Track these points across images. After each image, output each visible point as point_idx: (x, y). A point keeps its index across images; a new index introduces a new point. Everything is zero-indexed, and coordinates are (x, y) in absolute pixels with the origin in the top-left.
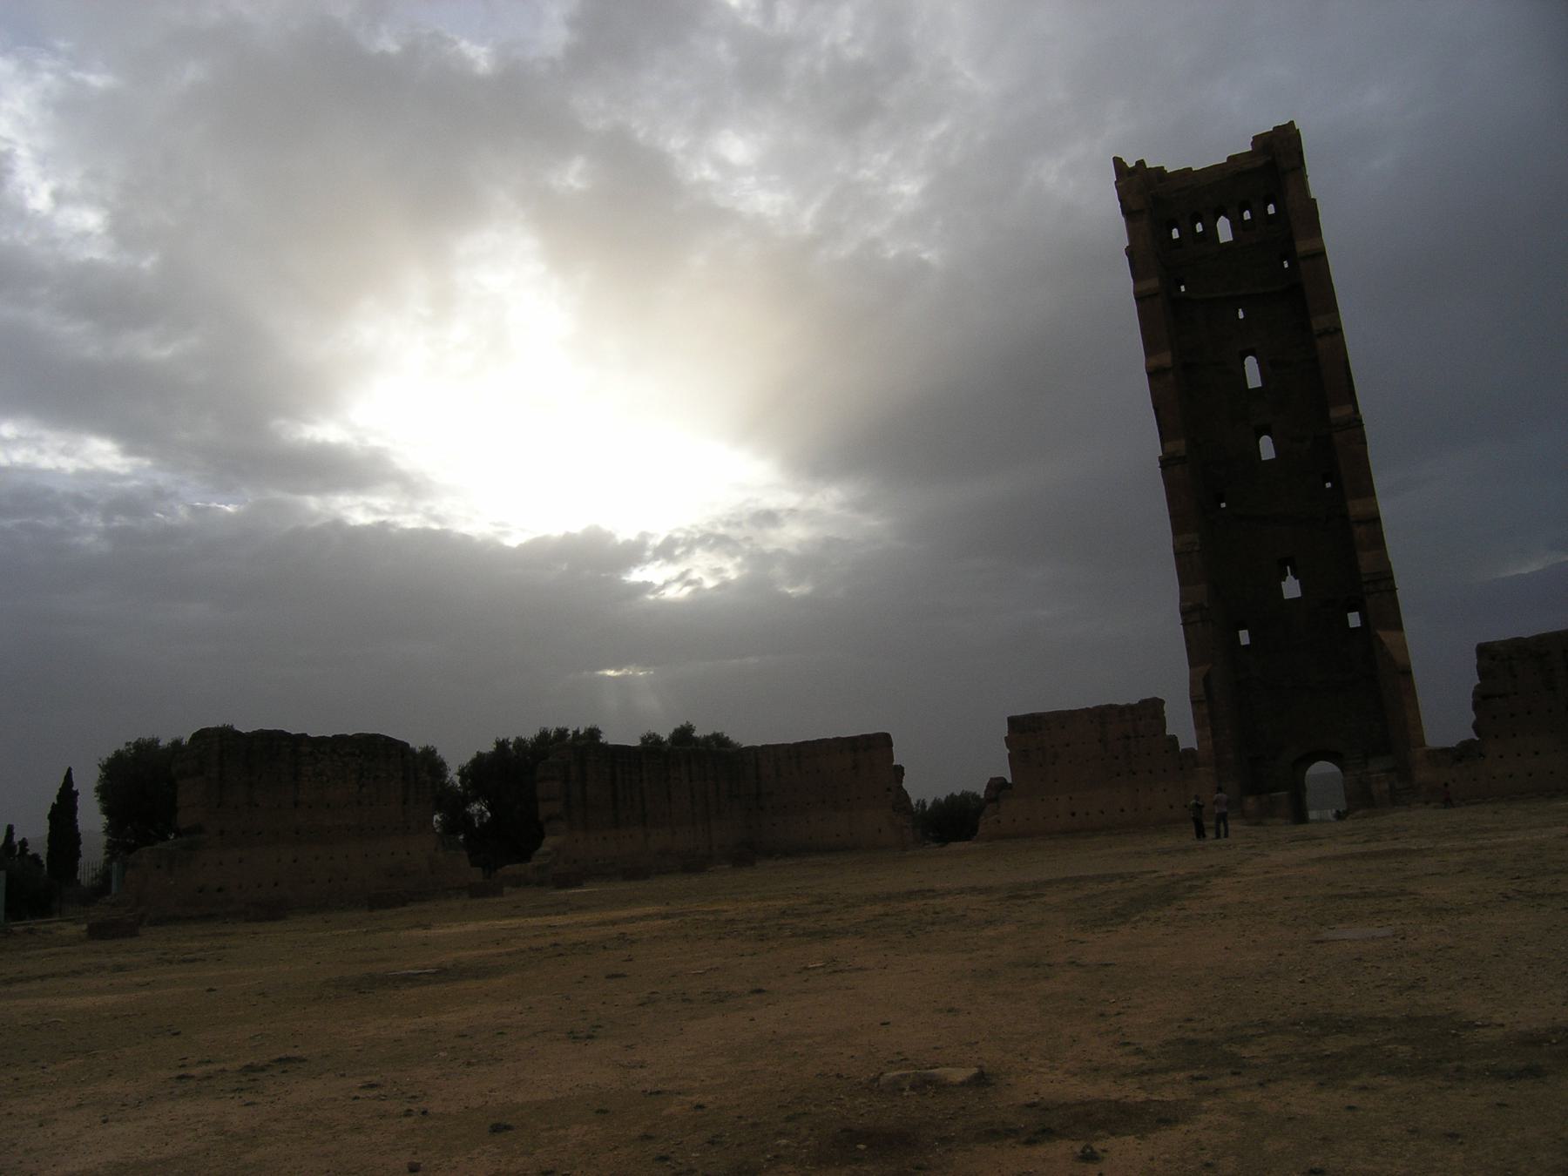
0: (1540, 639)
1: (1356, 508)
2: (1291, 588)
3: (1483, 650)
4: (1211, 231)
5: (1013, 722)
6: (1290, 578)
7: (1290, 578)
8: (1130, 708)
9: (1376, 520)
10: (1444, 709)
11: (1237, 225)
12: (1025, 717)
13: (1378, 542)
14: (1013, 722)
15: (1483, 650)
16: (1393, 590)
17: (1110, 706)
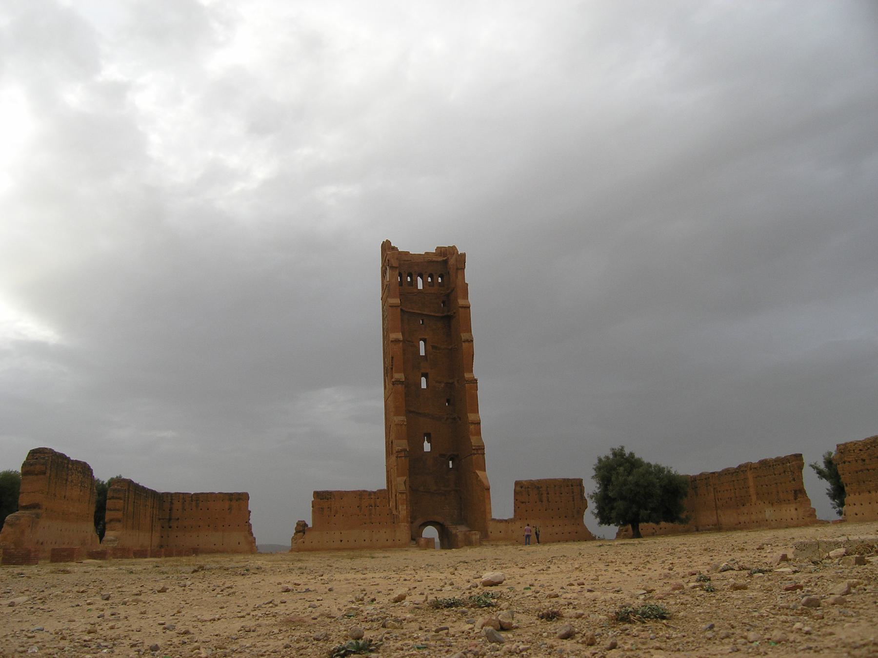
0: (539, 481)
1: (471, 417)
2: (427, 447)
3: (517, 483)
4: (413, 283)
5: (319, 496)
6: (426, 442)
7: (426, 442)
8: (374, 493)
9: (478, 423)
10: (502, 506)
11: (425, 282)
12: (324, 492)
13: (478, 433)
14: (317, 494)
15: (517, 483)
16: (484, 454)
17: (364, 491)
